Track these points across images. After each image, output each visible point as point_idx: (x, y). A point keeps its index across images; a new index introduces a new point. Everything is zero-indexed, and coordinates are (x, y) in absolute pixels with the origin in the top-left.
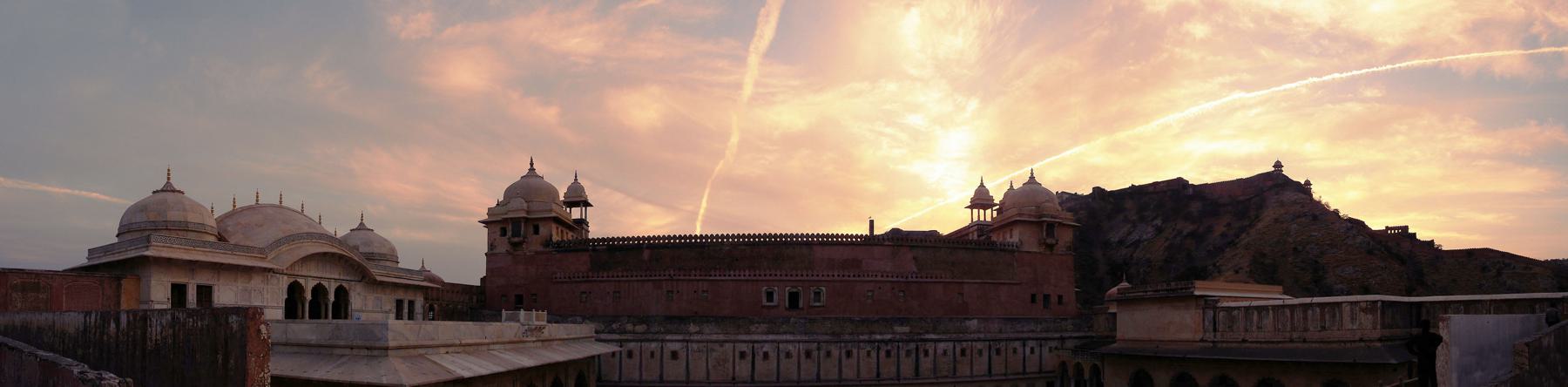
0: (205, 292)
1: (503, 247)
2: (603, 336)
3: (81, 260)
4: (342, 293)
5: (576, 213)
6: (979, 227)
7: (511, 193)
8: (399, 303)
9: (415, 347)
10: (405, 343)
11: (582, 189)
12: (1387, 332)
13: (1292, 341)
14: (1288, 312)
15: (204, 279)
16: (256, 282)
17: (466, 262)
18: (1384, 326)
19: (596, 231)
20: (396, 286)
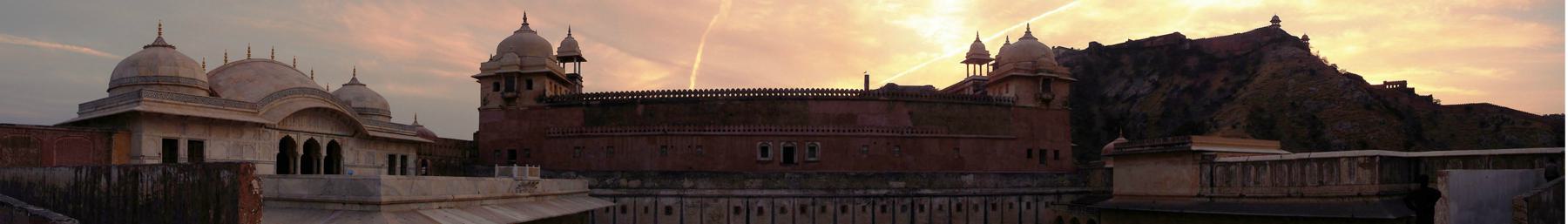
0: (196, 147)
1: (496, 103)
2: (597, 191)
3: (73, 115)
4: (334, 148)
5: (569, 68)
6: (975, 82)
7: (504, 47)
8: (392, 158)
9: (408, 202)
10: (397, 198)
11: (575, 44)
12: (1386, 187)
13: (1289, 196)
14: (1285, 167)
15: (195, 134)
16: (248, 136)
17: (458, 115)
18: (1381, 182)
19: (589, 85)
20: (388, 141)
